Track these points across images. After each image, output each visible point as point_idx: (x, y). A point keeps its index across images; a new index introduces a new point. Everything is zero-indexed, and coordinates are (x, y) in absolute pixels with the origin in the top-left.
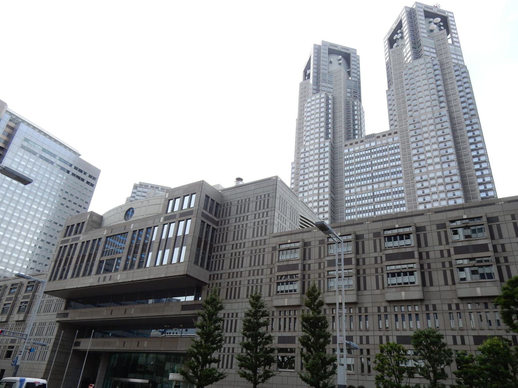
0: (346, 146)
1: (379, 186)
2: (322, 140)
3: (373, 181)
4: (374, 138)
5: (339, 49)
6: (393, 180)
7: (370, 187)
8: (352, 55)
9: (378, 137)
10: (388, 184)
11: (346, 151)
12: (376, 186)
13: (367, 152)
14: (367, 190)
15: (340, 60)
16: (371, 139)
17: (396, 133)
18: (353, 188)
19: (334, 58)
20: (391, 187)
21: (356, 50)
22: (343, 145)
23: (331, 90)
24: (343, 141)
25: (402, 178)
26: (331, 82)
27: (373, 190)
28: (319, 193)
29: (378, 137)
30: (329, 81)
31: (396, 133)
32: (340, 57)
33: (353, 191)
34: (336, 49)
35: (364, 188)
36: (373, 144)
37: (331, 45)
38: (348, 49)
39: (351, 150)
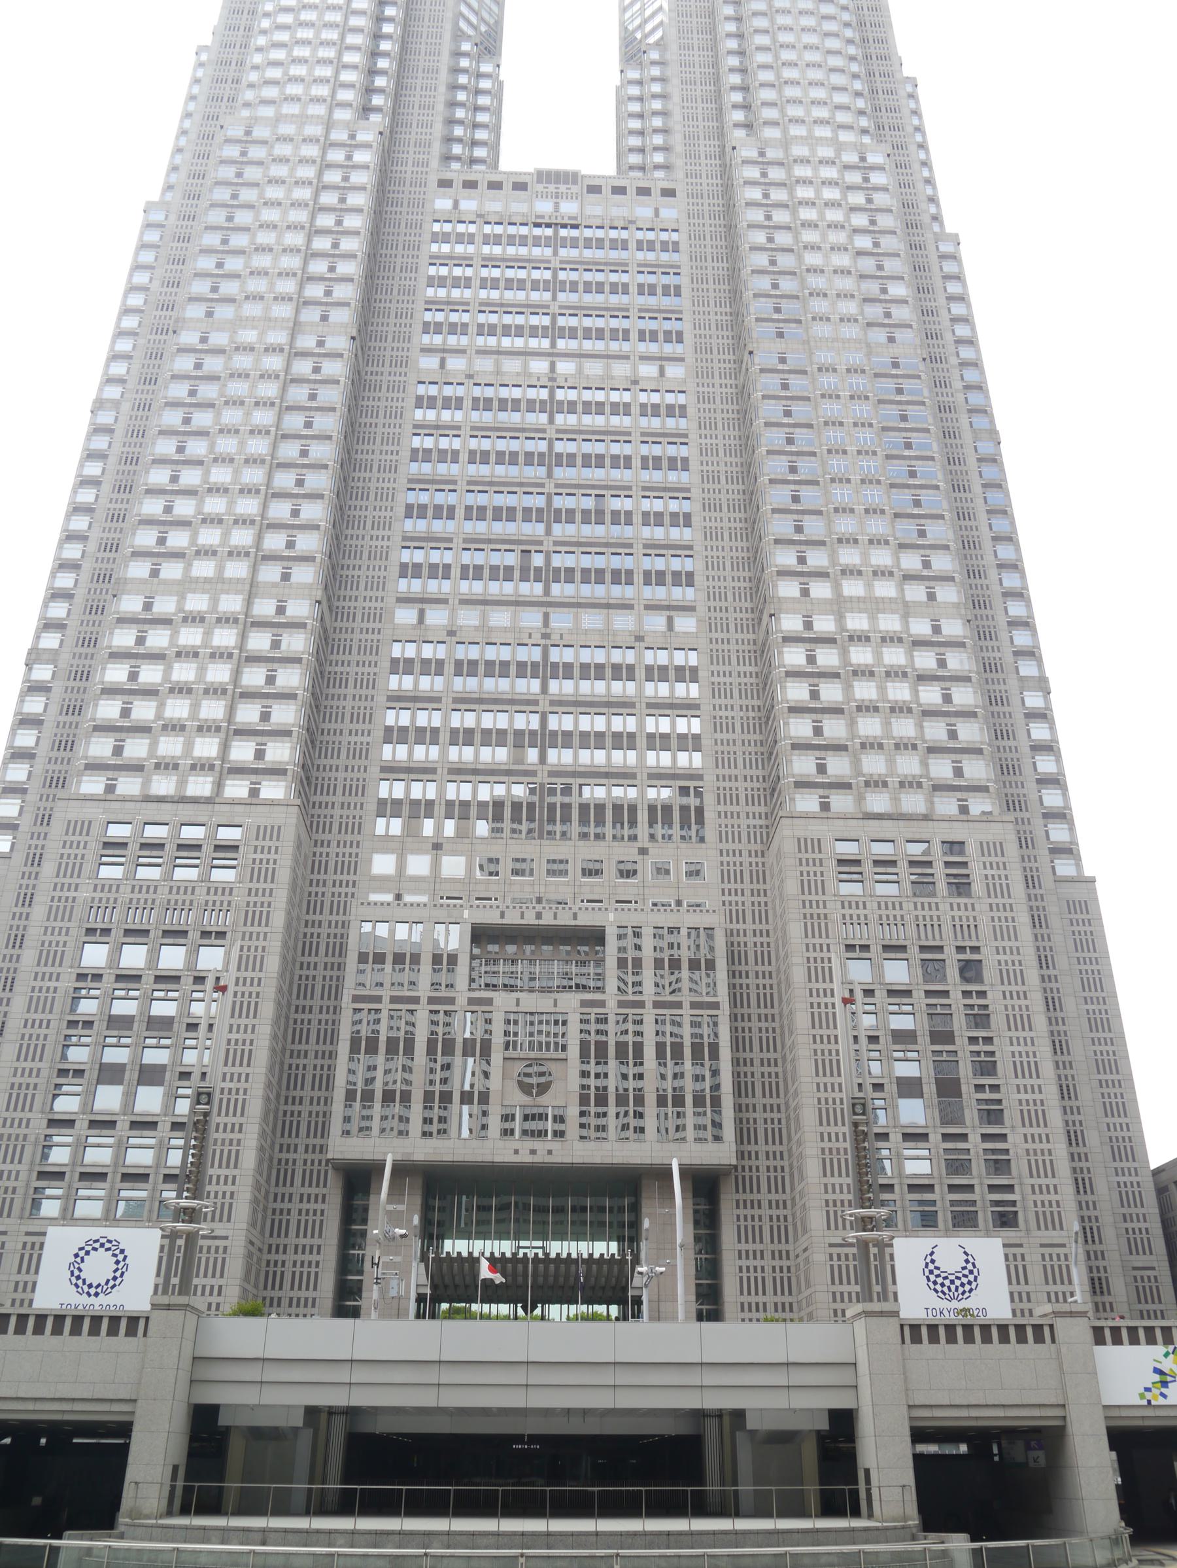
0: (445, 184)
1: (580, 370)
3: (553, 345)
4: (575, 189)
6: (645, 358)
9: (594, 189)
11: (443, 204)
13: (537, 231)
16: (563, 188)
18: (461, 351)
20: (635, 382)
22: (433, 179)
24: (435, 163)
25: (682, 360)
27: (552, 379)
28: (296, 323)
31: (669, 193)
36: (569, 208)
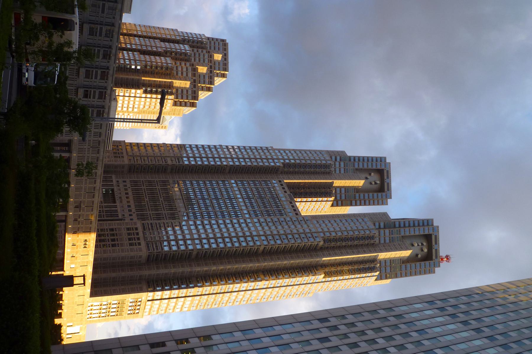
2: (282, 161)
5: (386, 180)
7: (239, 196)
8: (384, 194)
10: (244, 208)
12: (241, 200)
14: (236, 195)
15: (376, 183)
17: (297, 214)
19: (374, 177)
21: (391, 198)
23: (338, 171)
26: (347, 172)
29: (291, 203)
30: (347, 169)
32: (378, 182)
33: (234, 185)
34: (385, 177)
35: (237, 192)
36: (283, 199)
37: (388, 173)
38: (389, 189)
39: (276, 185)
